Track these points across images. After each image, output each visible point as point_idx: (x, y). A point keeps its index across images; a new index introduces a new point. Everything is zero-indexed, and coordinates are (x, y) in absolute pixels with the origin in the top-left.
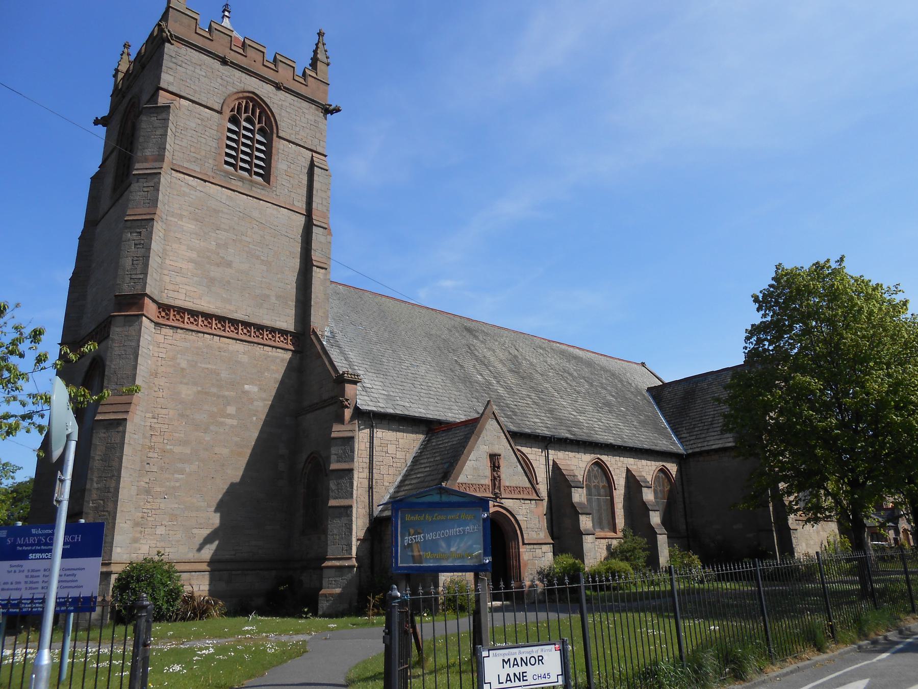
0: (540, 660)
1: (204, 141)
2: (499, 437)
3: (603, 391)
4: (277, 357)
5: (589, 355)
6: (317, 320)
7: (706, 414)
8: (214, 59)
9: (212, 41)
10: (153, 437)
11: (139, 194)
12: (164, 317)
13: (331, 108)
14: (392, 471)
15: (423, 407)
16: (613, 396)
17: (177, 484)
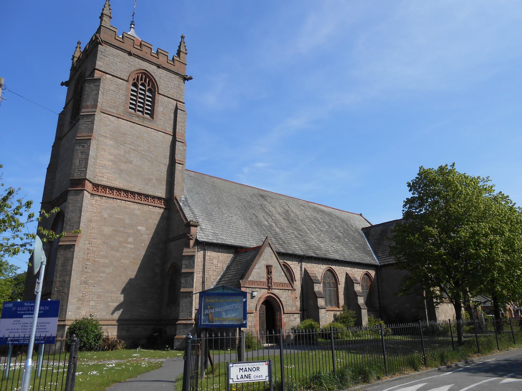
0: (258, 369)
1: (118, 96)
2: (272, 256)
3: (336, 230)
5: (330, 210)
6: (177, 192)
7: (392, 243)
8: (125, 52)
9: (124, 43)
10: (89, 254)
11: (83, 125)
12: (96, 190)
13: (187, 77)
14: (215, 273)
15: (233, 239)
16: (341, 233)
17: (101, 279)
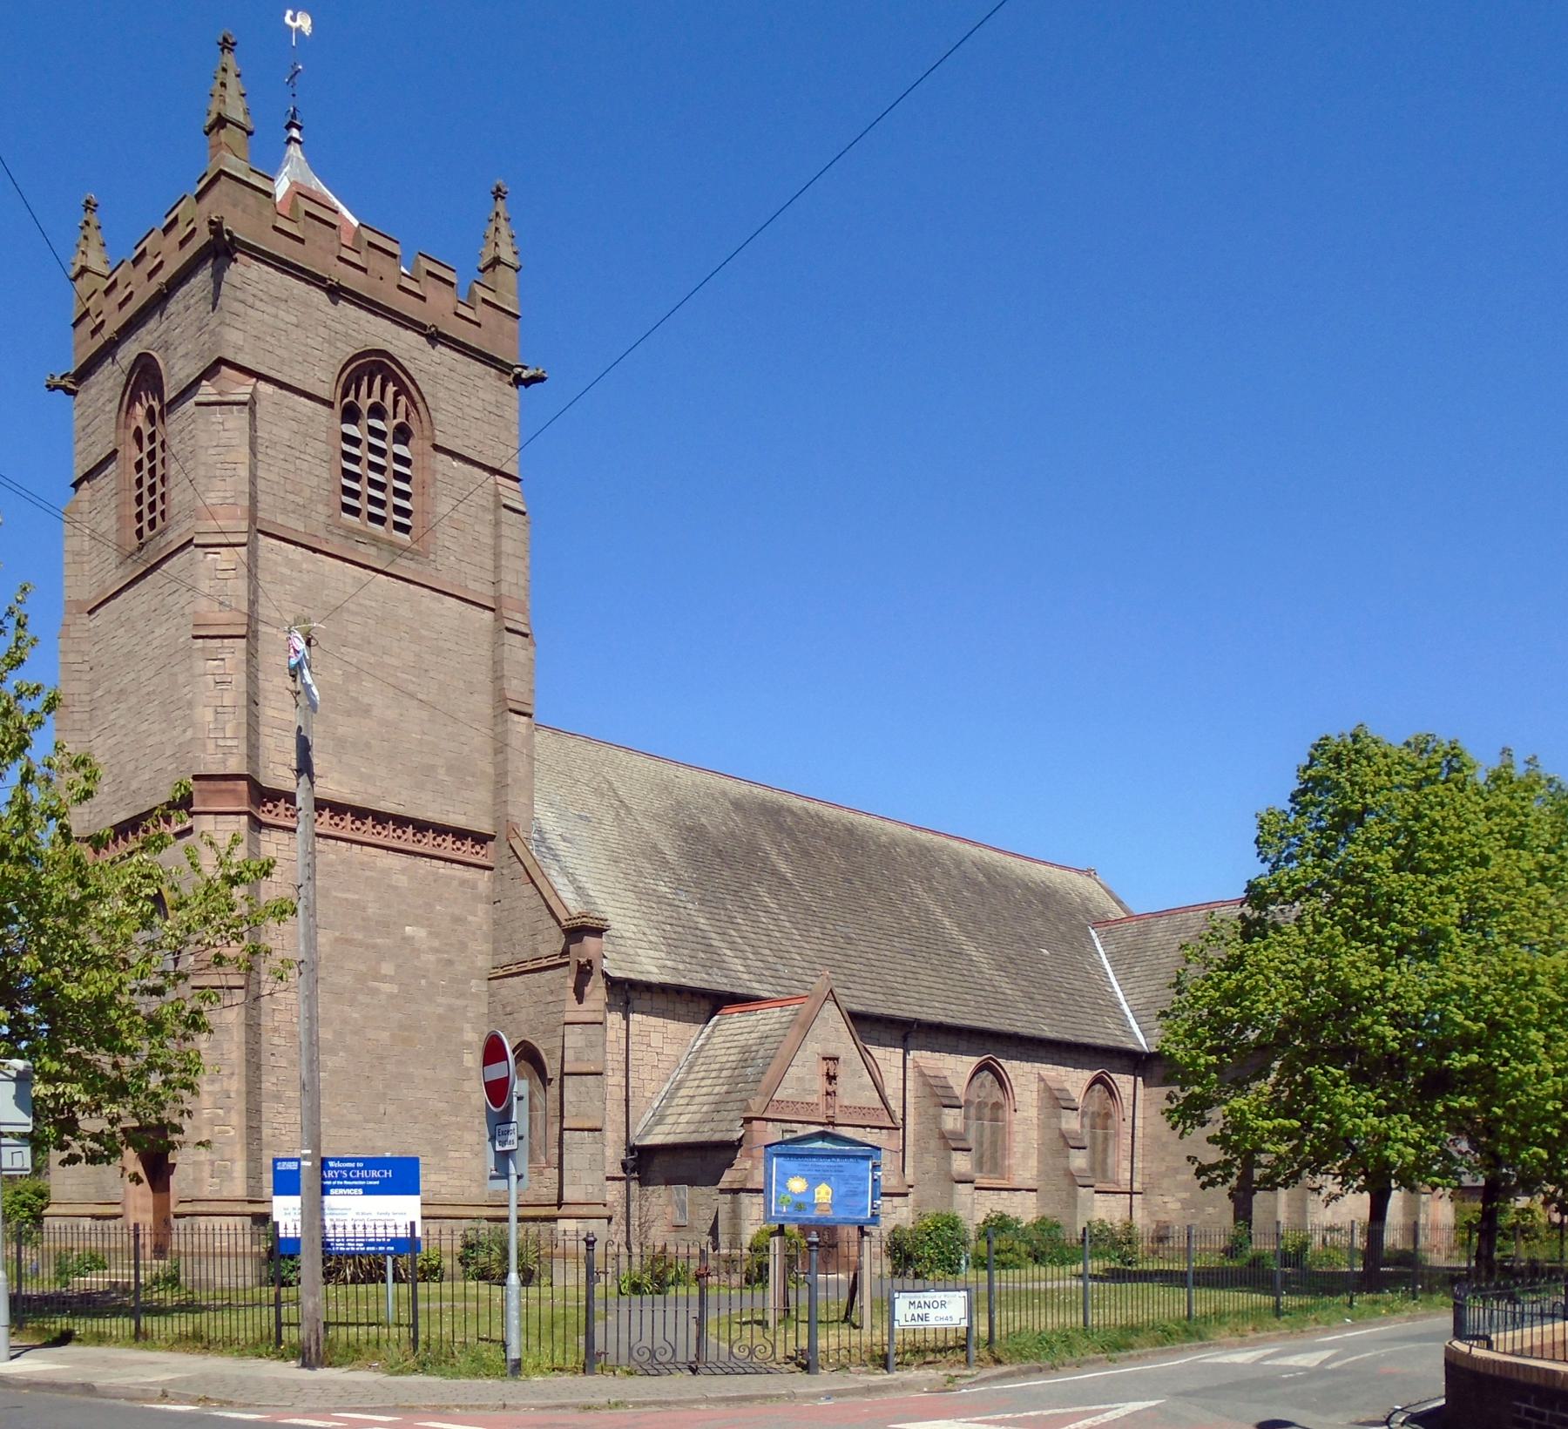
1: (305, 466)
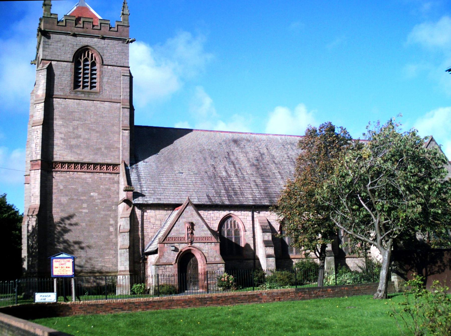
4: (107, 178)
